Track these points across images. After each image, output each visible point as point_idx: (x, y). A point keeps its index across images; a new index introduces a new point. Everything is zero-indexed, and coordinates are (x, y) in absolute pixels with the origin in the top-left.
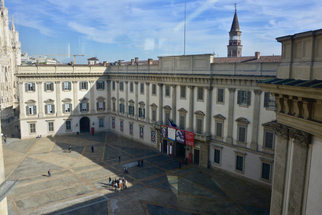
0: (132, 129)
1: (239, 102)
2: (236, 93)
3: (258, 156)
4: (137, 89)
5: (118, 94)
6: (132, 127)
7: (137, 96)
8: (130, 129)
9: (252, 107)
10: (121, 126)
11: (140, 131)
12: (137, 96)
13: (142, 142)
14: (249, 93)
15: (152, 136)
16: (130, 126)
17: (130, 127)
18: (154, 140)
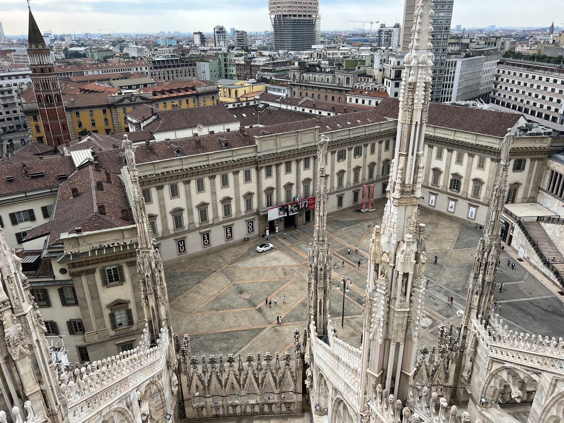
0: (208, 239)
1: (338, 160)
2: (336, 153)
3: (351, 191)
4: (213, 185)
5: (162, 207)
6: (208, 236)
7: (214, 193)
8: (204, 240)
9: (346, 161)
10: (179, 246)
11: (227, 233)
12: (214, 193)
13: (230, 243)
14: (345, 151)
15: (249, 227)
16: (204, 237)
17: (204, 238)
18: (253, 230)
